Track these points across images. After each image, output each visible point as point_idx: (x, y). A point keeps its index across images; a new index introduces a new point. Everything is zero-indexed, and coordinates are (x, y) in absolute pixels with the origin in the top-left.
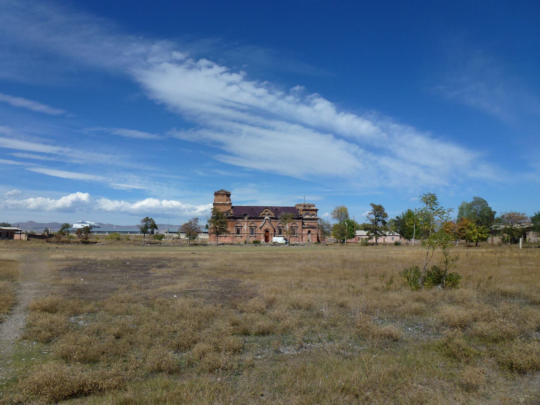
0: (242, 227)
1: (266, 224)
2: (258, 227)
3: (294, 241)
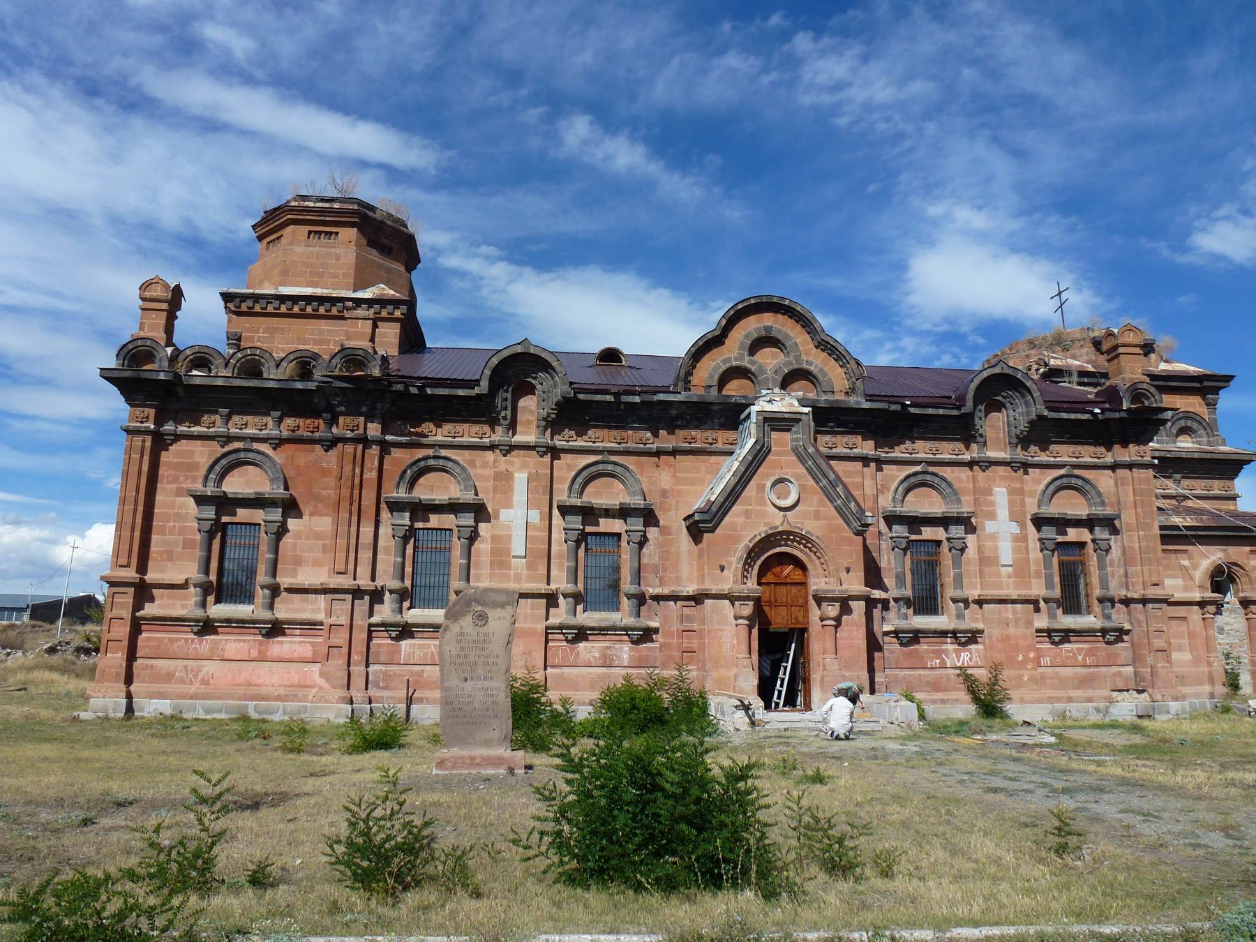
1: (764, 476)
2: (673, 518)
3: (1085, 682)
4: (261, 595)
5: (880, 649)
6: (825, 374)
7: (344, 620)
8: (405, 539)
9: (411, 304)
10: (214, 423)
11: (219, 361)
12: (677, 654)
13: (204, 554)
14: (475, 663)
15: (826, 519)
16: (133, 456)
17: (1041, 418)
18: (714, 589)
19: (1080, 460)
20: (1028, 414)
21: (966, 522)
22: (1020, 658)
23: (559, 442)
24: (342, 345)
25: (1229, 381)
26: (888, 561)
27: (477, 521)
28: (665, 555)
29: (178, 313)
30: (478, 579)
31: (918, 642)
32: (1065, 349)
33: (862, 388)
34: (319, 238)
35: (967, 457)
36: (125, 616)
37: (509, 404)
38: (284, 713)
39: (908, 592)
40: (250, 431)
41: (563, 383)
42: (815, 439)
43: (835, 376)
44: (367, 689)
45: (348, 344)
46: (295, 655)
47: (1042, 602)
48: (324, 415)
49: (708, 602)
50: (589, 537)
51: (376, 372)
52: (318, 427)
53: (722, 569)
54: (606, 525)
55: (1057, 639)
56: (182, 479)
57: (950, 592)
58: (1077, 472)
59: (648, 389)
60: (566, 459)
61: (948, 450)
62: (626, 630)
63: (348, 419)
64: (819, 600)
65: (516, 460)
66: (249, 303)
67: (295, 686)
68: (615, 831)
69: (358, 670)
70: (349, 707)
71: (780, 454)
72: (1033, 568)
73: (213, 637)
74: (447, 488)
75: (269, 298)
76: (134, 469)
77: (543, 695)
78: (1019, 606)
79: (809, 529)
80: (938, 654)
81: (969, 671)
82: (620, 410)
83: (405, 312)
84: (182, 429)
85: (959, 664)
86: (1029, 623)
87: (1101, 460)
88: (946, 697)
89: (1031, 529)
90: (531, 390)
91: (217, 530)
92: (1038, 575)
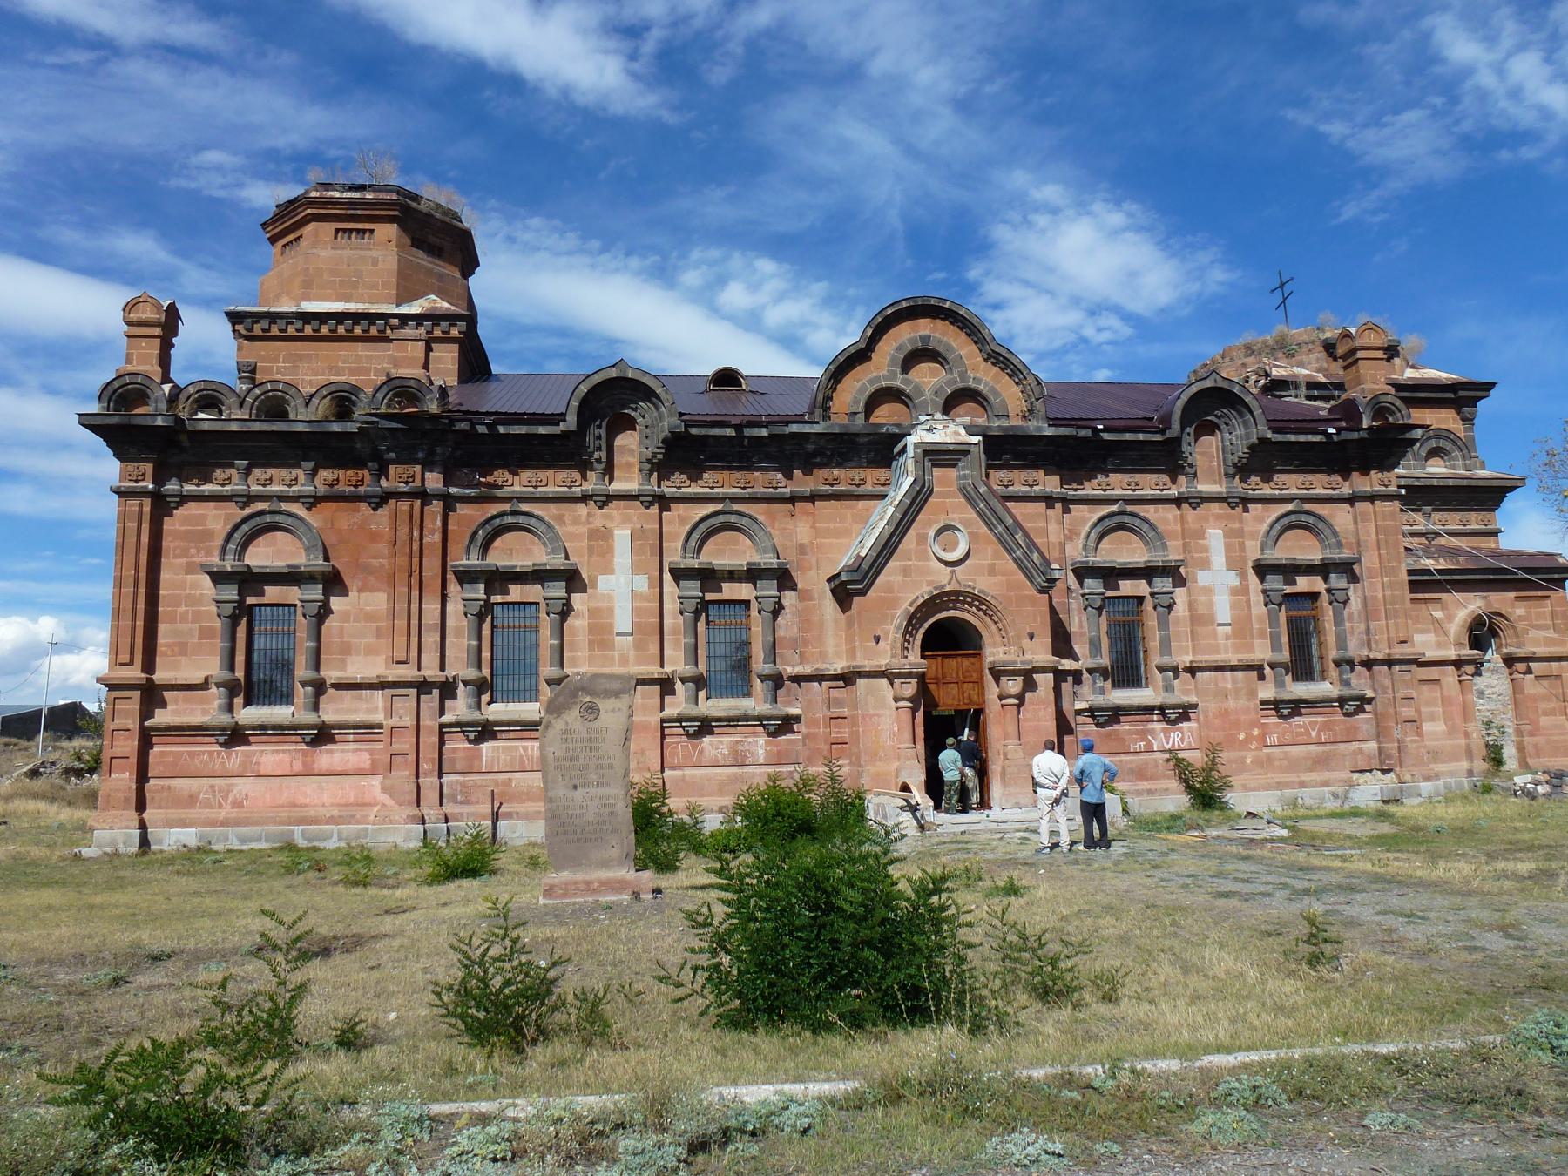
0: (572, 579)
1: (926, 524)
2: (814, 581)
3: (1321, 762)
4: (302, 693)
5: (1071, 731)
6: (997, 394)
7: (409, 721)
8: (481, 617)
9: (471, 318)
10: (230, 479)
11: (232, 400)
12: (824, 747)
13: (227, 644)
14: (585, 767)
15: (1003, 575)
16: (128, 524)
17: (1263, 441)
18: (868, 665)
19: (1311, 492)
20: (1248, 436)
21: (1173, 572)
22: (1242, 736)
23: (668, 489)
24: (388, 374)
25: (1489, 390)
26: (1078, 623)
27: (569, 591)
28: (806, 624)
29: (175, 340)
30: (574, 662)
31: (1118, 722)
32: (1290, 355)
33: (1043, 410)
34: (349, 238)
35: (1173, 492)
36: (131, 726)
37: (603, 443)
38: (340, 839)
39: (1105, 660)
40: (276, 488)
41: (671, 415)
42: (987, 475)
43: (1010, 396)
44: (441, 804)
45: (395, 373)
46: (350, 767)
47: (1267, 667)
48: (370, 464)
49: (861, 682)
50: (710, 607)
51: (433, 407)
52: (362, 480)
53: (877, 639)
54: (731, 591)
55: (1286, 712)
56: (193, 551)
57: (1156, 659)
58: (1307, 507)
59: (776, 418)
60: (678, 510)
61: (1150, 484)
62: (760, 719)
63: (401, 469)
64: (997, 674)
65: (615, 513)
66: (264, 324)
67: (351, 805)
68: (784, 961)
69: (429, 782)
70: (421, 827)
71: (943, 495)
72: (1256, 626)
73: (243, 748)
74: (529, 551)
75: (289, 318)
76: (131, 541)
77: (664, 804)
78: (1239, 674)
79: (982, 588)
80: (1143, 734)
81: (1181, 755)
82: (743, 446)
83: (464, 329)
84: (189, 488)
85: (1168, 747)
86: (1252, 693)
87: (1337, 492)
88: (1153, 787)
89: (1253, 578)
90: (630, 424)
91: (241, 614)
92: (1262, 635)
